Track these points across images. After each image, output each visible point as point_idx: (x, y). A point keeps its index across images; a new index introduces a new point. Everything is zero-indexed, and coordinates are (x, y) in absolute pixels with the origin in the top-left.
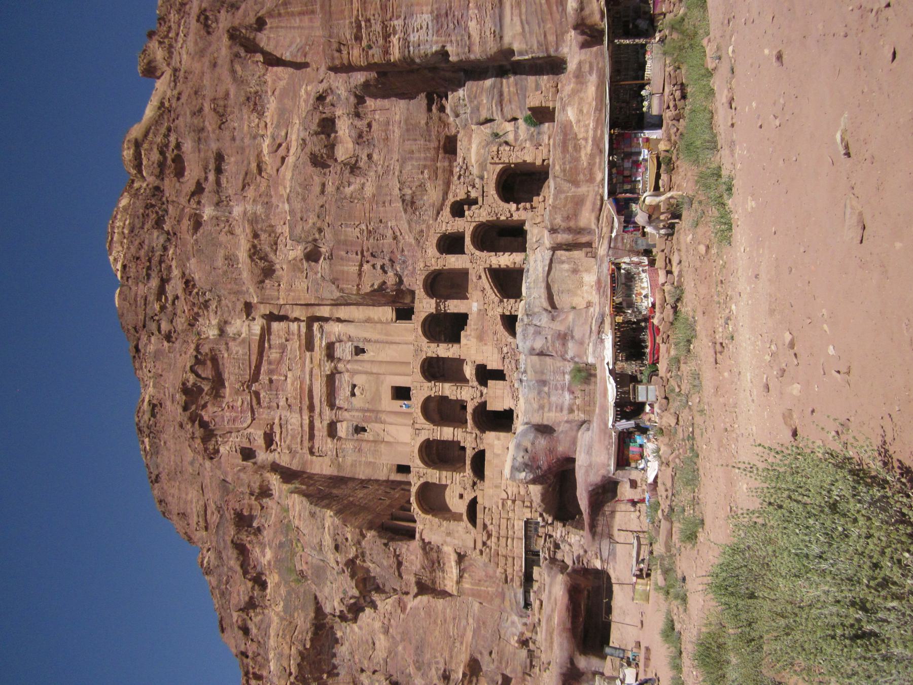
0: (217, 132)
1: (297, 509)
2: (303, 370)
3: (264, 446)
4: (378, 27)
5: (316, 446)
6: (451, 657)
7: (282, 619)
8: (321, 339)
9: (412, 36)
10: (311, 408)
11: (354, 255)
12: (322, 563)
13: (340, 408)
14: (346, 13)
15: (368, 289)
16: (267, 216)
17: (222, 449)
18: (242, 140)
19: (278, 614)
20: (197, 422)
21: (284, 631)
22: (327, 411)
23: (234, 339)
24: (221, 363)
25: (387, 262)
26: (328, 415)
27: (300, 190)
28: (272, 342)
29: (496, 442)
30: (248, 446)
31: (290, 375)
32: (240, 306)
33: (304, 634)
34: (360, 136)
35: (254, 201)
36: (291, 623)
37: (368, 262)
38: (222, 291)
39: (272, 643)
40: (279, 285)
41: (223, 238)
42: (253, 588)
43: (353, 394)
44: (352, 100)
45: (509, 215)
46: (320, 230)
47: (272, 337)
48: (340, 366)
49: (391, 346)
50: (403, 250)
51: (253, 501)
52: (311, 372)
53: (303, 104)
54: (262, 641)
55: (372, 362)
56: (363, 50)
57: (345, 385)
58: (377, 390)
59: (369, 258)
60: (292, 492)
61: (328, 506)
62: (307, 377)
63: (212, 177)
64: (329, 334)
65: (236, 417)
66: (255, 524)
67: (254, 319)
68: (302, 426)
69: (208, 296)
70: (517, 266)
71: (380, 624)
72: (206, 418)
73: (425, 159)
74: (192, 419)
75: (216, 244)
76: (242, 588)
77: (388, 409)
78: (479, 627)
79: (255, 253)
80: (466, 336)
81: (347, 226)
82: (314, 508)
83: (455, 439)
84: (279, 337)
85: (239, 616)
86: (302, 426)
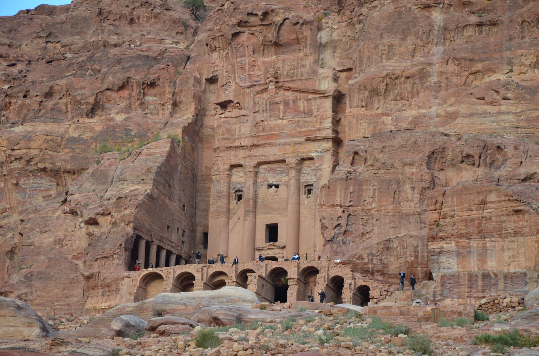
0: (520, 20)
1: (157, 151)
3: (220, 101)
5: (221, 154)
6: (37, 305)
9: (444, 257)
11: (349, 199)
12: (110, 180)
14: (460, 207)
16: (427, 88)
17: (215, 55)
18: (509, 49)
19: (66, 131)
21: (52, 140)
22: (254, 162)
23: (316, 62)
30: (220, 83)
33: (50, 161)
35: (442, 73)
37: (344, 212)
38: (362, 44)
39: (41, 127)
40: (363, 107)
41: (410, 40)
42: (88, 103)
43: (270, 186)
46: (372, 166)
47: (319, 101)
49: (313, 220)
50: (353, 242)
52: (289, 144)
54: (41, 114)
55: (299, 204)
56: (436, 221)
57: (278, 178)
59: (346, 213)
60: (172, 142)
61: (156, 183)
62: (282, 141)
64: (321, 158)
65: (245, 70)
67: (336, 79)
68: (238, 138)
71: (62, 237)
73: (422, 257)
76: (87, 92)
77: (258, 221)
79: (392, 79)
81: (374, 190)
82: (154, 171)
84: (318, 109)
85: (62, 87)
86: (238, 138)
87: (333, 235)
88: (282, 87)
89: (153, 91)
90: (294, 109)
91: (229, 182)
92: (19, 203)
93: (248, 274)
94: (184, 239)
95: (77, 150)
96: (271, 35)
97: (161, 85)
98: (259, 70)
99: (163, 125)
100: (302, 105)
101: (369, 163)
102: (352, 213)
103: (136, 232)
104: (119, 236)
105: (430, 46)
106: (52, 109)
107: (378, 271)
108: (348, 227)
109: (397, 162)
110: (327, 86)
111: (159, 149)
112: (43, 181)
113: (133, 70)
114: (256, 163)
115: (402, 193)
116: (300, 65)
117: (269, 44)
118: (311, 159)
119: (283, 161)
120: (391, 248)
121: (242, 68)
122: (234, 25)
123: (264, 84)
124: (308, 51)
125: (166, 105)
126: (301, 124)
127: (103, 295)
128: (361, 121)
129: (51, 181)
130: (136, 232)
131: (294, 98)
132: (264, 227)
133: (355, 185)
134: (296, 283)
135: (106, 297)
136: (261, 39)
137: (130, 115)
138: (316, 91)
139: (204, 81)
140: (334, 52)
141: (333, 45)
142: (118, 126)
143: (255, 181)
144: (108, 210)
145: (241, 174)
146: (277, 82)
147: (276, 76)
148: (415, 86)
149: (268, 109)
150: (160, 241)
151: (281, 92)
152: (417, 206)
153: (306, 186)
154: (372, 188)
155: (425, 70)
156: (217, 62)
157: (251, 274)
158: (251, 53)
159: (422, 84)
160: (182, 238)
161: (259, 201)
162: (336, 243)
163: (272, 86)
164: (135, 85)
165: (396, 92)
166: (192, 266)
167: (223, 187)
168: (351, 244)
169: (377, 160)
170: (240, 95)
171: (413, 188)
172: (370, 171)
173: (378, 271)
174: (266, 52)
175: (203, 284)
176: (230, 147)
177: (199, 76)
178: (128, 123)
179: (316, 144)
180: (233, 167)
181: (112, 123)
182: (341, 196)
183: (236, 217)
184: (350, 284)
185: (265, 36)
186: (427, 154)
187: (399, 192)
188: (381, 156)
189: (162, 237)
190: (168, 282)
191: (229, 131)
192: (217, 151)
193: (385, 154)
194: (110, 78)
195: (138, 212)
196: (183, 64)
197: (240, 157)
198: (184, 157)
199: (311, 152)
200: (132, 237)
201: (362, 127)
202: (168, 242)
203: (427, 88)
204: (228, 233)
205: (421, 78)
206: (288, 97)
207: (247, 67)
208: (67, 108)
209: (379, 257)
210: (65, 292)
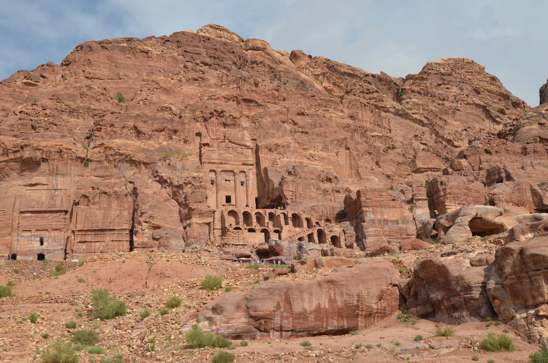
2: (234, 161)
4: (370, 205)
10: (221, 163)
15: (285, 194)
16: (290, 152)
17: (198, 124)
20: (210, 116)
22: (221, 170)
25: (294, 200)
26: (219, 170)
31: (232, 156)
32: (255, 137)
34: (327, 191)
41: (280, 132)
43: (226, 180)
44: (337, 189)
47: (246, 150)
48: (237, 176)
51: (182, 137)
53: (327, 167)
63: (300, 130)
66: (174, 137)
69: (257, 124)
72: (212, 119)
74: (211, 113)
75: (278, 130)
78: (173, 230)
79: (277, 146)
84: (246, 153)
92: (116, 174)
121: (212, 131)
124: (240, 129)
165: (278, 151)
176: (210, 163)
180: (211, 171)
183: (212, 191)
203: (290, 152)
205: (288, 147)
207: (215, 131)
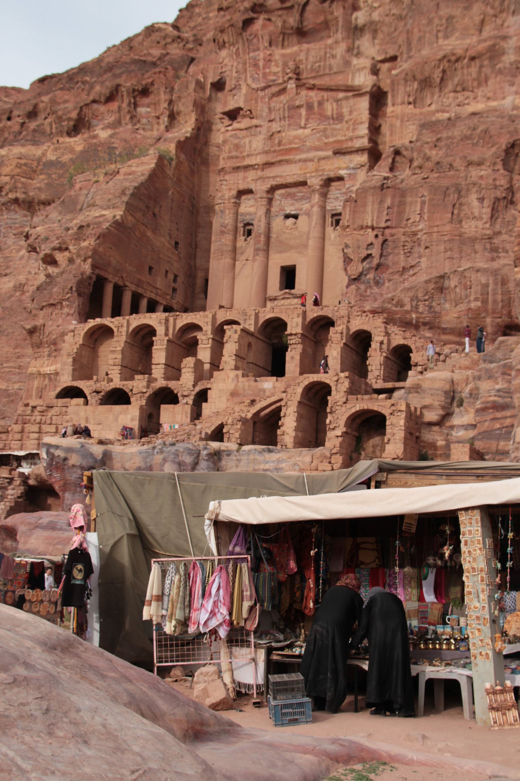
3: (227, 109)
5: (227, 177)
7: (39, 160)
8: (348, 168)
10: (269, 164)
11: (385, 218)
12: (79, 207)
13: (270, 201)
16: (500, 72)
17: (224, 53)
19: (44, 154)
21: (25, 165)
22: (267, 186)
23: (350, 50)
24: (324, 34)
27: (479, 130)
28: (344, 103)
29: (129, 417)
30: (228, 87)
31: (307, 131)
33: (23, 190)
36: (35, 171)
37: (376, 236)
40: (410, 103)
41: (477, 9)
42: (69, 119)
43: (287, 217)
45: (332, 426)
46: (420, 167)
47: (352, 101)
50: (390, 280)
52: (311, 160)
54: (21, 136)
55: (323, 239)
57: (297, 205)
58: (292, 247)
62: (303, 156)
65: (258, 68)
67: (375, 71)
68: (248, 156)
70: (279, 438)
71: (23, 281)
77: (271, 263)
78: (9, 396)
79: (452, 60)
80: (237, 376)
81: (423, 203)
82: (129, 192)
83: (153, 367)
84: (351, 112)
86: (248, 156)
87: (361, 270)
88: (304, 84)
89: (146, 101)
90: (320, 114)
91: (237, 213)
93: (225, 327)
94: (176, 286)
95: (54, 176)
96: (292, 21)
97: (155, 92)
98: (277, 66)
99: (154, 141)
100: (329, 108)
101: (415, 164)
102: (390, 239)
103: (97, 271)
104: (71, 276)
105: (504, 15)
106: (34, 131)
107: (425, 324)
108: (383, 259)
109: (458, 159)
110: (364, 80)
111: (143, 167)
112: (17, 216)
113: (124, 76)
114: (269, 186)
115: (465, 207)
116: (328, 55)
117: (290, 32)
118: (340, 179)
119: (304, 184)
120: (447, 289)
121: (256, 66)
122: (246, 10)
123: (281, 84)
124: (339, 36)
125: (161, 117)
126: (328, 132)
127: (49, 356)
128: (408, 123)
129: (25, 216)
130: (97, 271)
131: (320, 99)
132: (278, 271)
133: (393, 197)
134: (300, 340)
135: (53, 358)
136: (280, 25)
137: (117, 130)
138: (347, 86)
139: (209, 86)
140: (374, 38)
141: (372, 28)
142: (102, 144)
143: (268, 211)
144: (65, 243)
145: (252, 202)
146: (298, 79)
147: (297, 71)
148: (484, 70)
149: (286, 115)
150: (138, 285)
151: (304, 92)
152: (487, 226)
153: (333, 215)
154: (419, 199)
155: (497, 47)
156: (225, 62)
157: (229, 327)
158: (266, 44)
159: (493, 66)
160: (173, 285)
161: (273, 236)
162: (364, 282)
163: (291, 85)
164: (125, 93)
165: (456, 80)
166: (154, 315)
167: (228, 219)
168: (387, 284)
169: (428, 159)
170: (252, 100)
171: (481, 200)
172: (416, 176)
173: (425, 324)
174: (286, 43)
175: (165, 342)
176: (238, 168)
177: (202, 80)
178: (113, 140)
179: (347, 157)
180: (241, 193)
181: (94, 141)
182: (373, 213)
183: (243, 257)
184: (382, 343)
185: (284, 22)
186: (504, 147)
187: (461, 204)
188: (434, 152)
189: (140, 280)
190: (119, 339)
191: (237, 147)
192: (222, 173)
193: (441, 149)
194: (98, 88)
195: (99, 245)
196: (186, 67)
197: (249, 180)
198: (179, 180)
199: (340, 169)
200: (90, 278)
201: (408, 131)
202: (150, 288)
203: (500, 72)
204: (234, 278)
205: (491, 58)
206: (311, 97)
208: (51, 129)
209: (427, 303)
210: (17, 351)
